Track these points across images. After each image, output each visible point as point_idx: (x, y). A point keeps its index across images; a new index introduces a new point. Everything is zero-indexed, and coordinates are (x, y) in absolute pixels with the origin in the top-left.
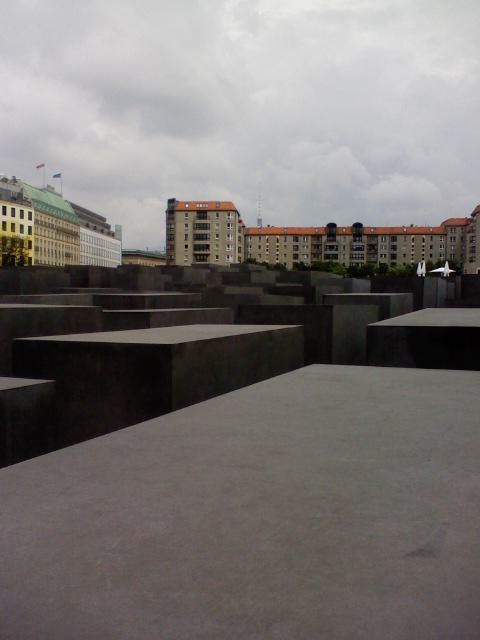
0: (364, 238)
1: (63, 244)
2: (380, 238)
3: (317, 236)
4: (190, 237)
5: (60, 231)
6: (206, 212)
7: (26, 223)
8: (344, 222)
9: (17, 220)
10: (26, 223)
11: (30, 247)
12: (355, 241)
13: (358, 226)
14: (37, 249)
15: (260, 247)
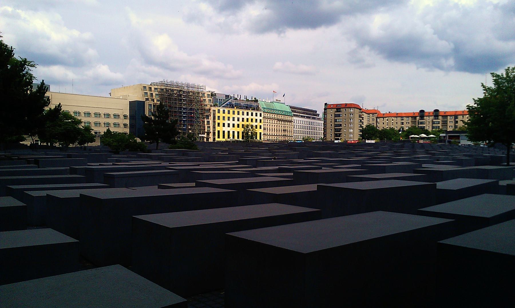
0: (440, 117)
1: (281, 126)
2: (449, 117)
3: (414, 117)
4: (333, 121)
5: (279, 120)
6: (340, 109)
7: (258, 118)
8: (429, 109)
9: (254, 117)
10: (258, 118)
11: (260, 128)
12: (435, 119)
13: (436, 111)
14: (264, 129)
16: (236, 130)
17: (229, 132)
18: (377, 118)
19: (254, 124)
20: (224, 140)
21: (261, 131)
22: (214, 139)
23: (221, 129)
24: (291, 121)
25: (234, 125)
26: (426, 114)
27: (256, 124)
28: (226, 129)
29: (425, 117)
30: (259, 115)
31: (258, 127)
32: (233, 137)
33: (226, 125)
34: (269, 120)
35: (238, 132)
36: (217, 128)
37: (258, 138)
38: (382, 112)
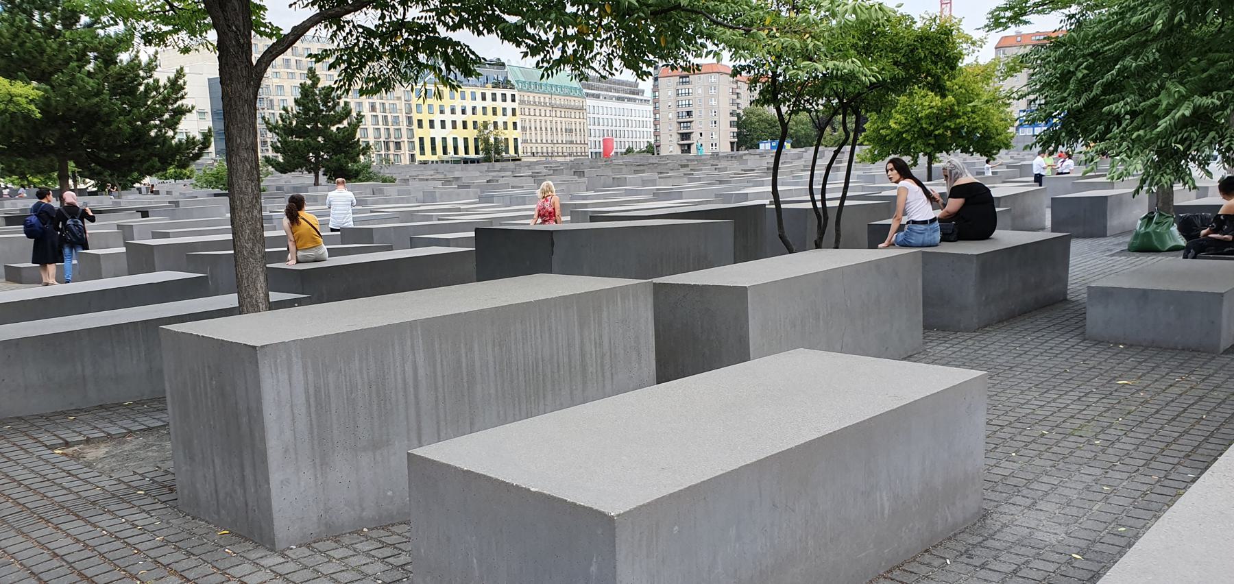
1: (561, 120)
7: (509, 105)
9: (499, 104)
11: (515, 128)
14: (524, 129)
16: (460, 134)
17: (444, 139)
19: (500, 119)
20: (435, 158)
21: (517, 134)
22: (412, 157)
23: (426, 133)
24: (582, 109)
25: (454, 124)
27: (505, 119)
28: (438, 133)
30: (509, 98)
31: (510, 126)
32: (456, 152)
33: (437, 124)
34: (532, 108)
35: (466, 140)
36: (419, 133)
37: (512, 151)
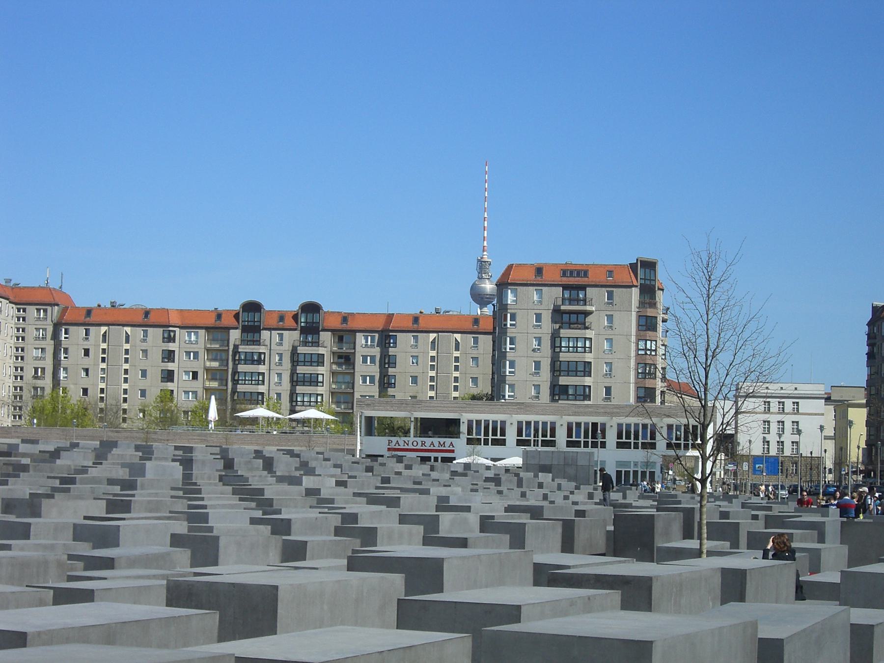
0: (326, 337)
3: (216, 328)
8: (280, 299)
13: (311, 308)
15: (87, 352)
18: (57, 326)
26: (266, 321)
29: (265, 334)
38: (82, 300)
